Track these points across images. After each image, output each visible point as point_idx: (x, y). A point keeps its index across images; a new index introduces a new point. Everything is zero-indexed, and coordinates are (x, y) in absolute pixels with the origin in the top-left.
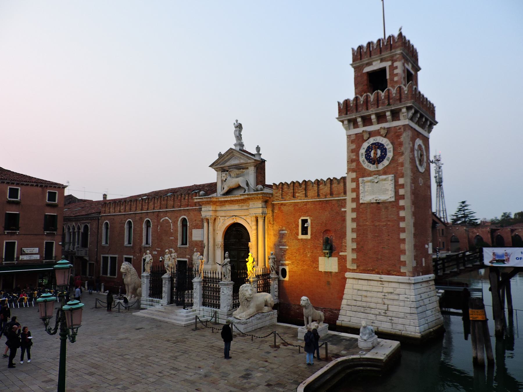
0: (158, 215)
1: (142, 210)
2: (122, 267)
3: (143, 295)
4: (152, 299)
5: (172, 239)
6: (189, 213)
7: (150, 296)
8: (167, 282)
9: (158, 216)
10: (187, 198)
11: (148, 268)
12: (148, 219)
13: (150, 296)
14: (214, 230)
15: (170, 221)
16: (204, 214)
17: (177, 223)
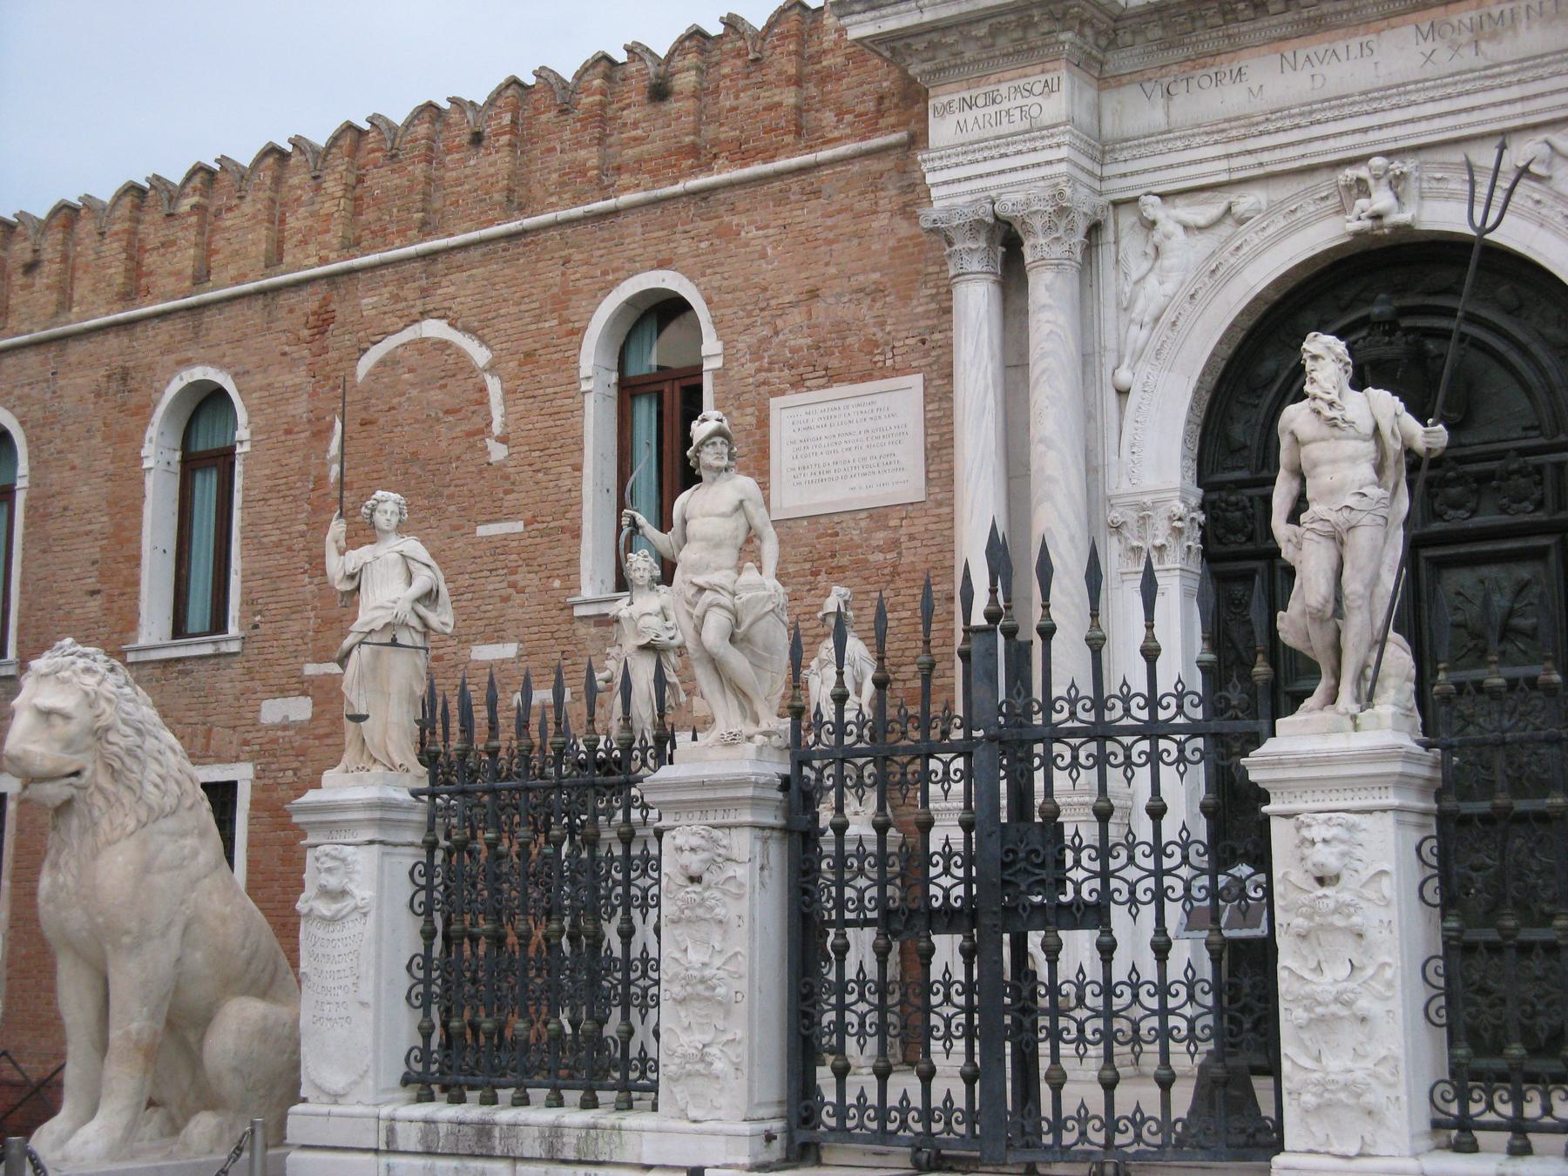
0: (325, 315)
1: (128, 296)
2: (35, 694)
3: (318, 1070)
4: (472, 1111)
5: (499, 546)
6: (728, 234)
7: (422, 1081)
8: (742, 844)
9: (323, 322)
10: (685, 81)
11: (386, 700)
12: (199, 373)
13: (422, 1081)
14: (1088, 359)
15: (480, 355)
16: (955, 185)
17: (572, 362)
